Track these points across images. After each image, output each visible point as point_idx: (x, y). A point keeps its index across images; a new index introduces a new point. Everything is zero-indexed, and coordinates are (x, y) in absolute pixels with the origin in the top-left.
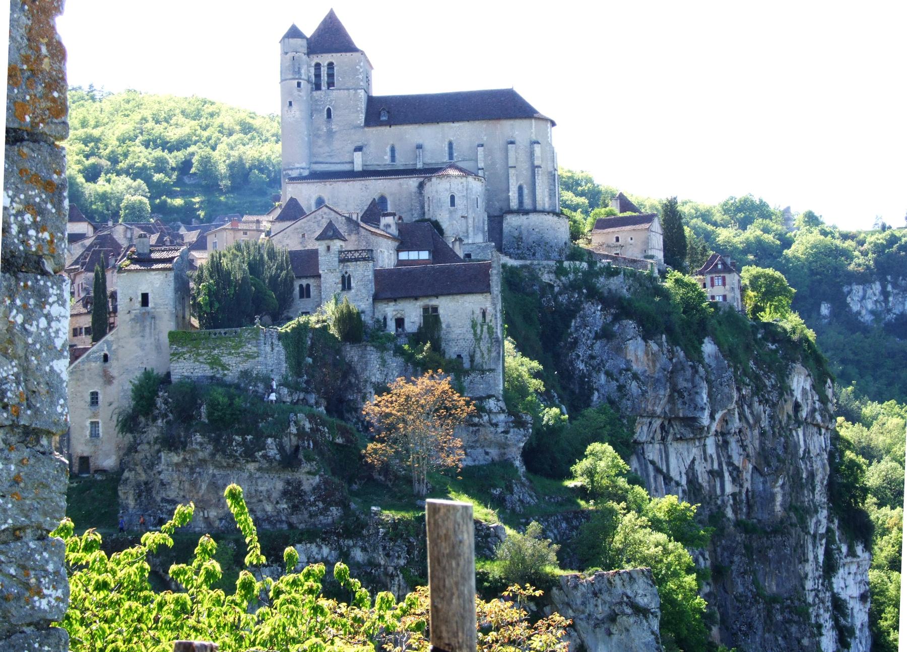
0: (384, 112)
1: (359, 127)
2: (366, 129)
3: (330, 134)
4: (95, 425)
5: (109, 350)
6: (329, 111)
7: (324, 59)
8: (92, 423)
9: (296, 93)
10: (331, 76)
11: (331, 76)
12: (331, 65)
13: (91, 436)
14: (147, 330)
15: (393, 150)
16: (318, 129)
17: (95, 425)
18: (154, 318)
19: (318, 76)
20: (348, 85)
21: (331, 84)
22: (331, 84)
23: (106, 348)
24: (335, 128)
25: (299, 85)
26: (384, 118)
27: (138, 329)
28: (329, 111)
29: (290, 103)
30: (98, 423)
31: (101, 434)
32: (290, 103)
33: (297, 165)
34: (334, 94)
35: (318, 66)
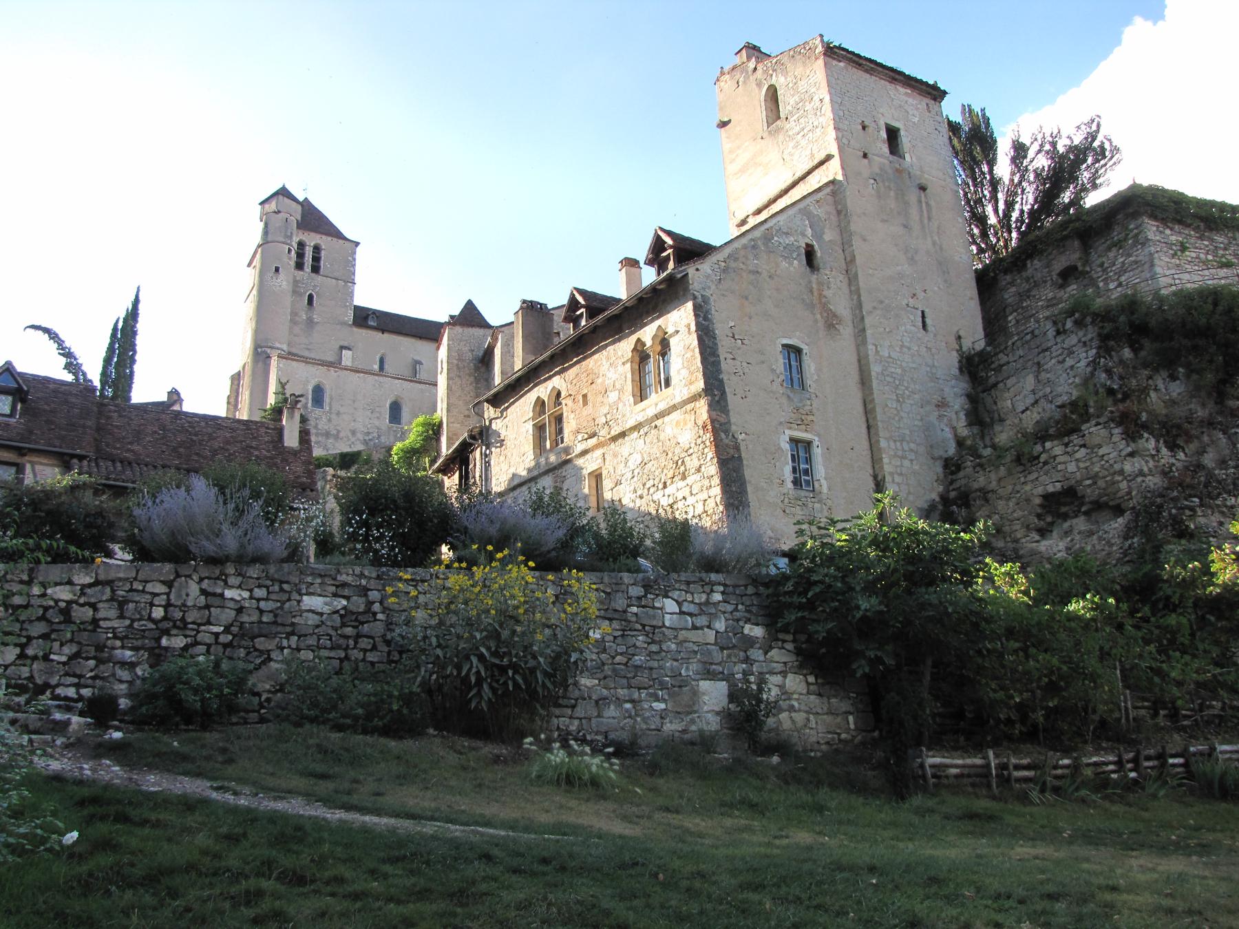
0: (364, 317)
1: (344, 323)
2: (355, 329)
3: (310, 323)
4: (801, 448)
5: (818, 235)
6: (311, 298)
7: (311, 239)
8: (794, 441)
9: (286, 260)
10: (316, 259)
11: (316, 259)
12: (317, 249)
13: (796, 482)
14: (914, 212)
15: (382, 361)
16: (296, 314)
17: (801, 448)
18: (923, 188)
19: (300, 255)
20: (336, 274)
21: (316, 269)
22: (316, 269)
23: (809, 232)
24: (316, 318)
25: (290, 250)
26: (371, 323)
27: (892, 204)
28: (311, 298)
29: (277, 270)
30: (808, 444)
31: (823, 486)
32: (277, 270)
33: (278, 345)
34: (318, 279)
35: (301, 245)
